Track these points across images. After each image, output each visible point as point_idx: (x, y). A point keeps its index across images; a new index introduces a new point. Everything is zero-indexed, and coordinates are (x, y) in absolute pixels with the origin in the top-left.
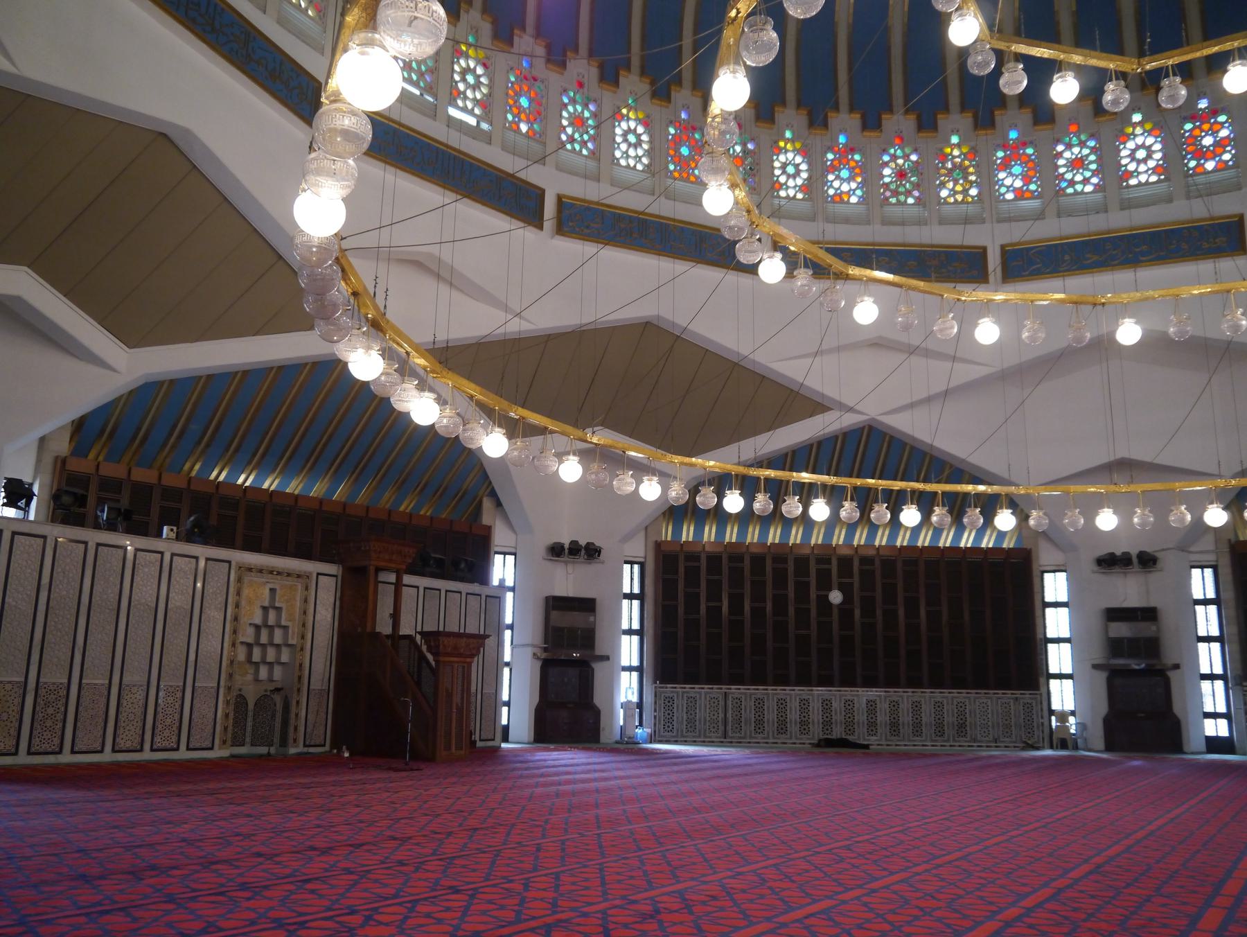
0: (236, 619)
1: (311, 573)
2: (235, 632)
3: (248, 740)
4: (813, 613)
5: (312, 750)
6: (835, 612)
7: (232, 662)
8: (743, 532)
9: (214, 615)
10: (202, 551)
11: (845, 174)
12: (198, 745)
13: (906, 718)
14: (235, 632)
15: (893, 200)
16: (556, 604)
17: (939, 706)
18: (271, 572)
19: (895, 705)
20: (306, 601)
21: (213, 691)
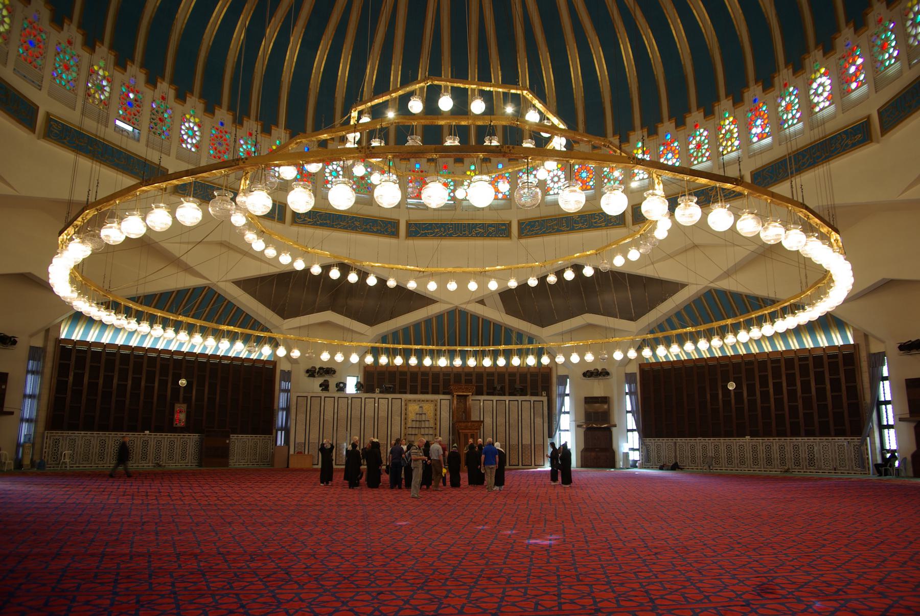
4: (720, 396)
6: (732, 393)
8: (786, 343)
9: (397, 419)
10: (390, 396)
11: (670, 156)
13: (776, 455)
15: (696, 162)
16: (589, 400)
17: (796, 447)
19: (769, 447)
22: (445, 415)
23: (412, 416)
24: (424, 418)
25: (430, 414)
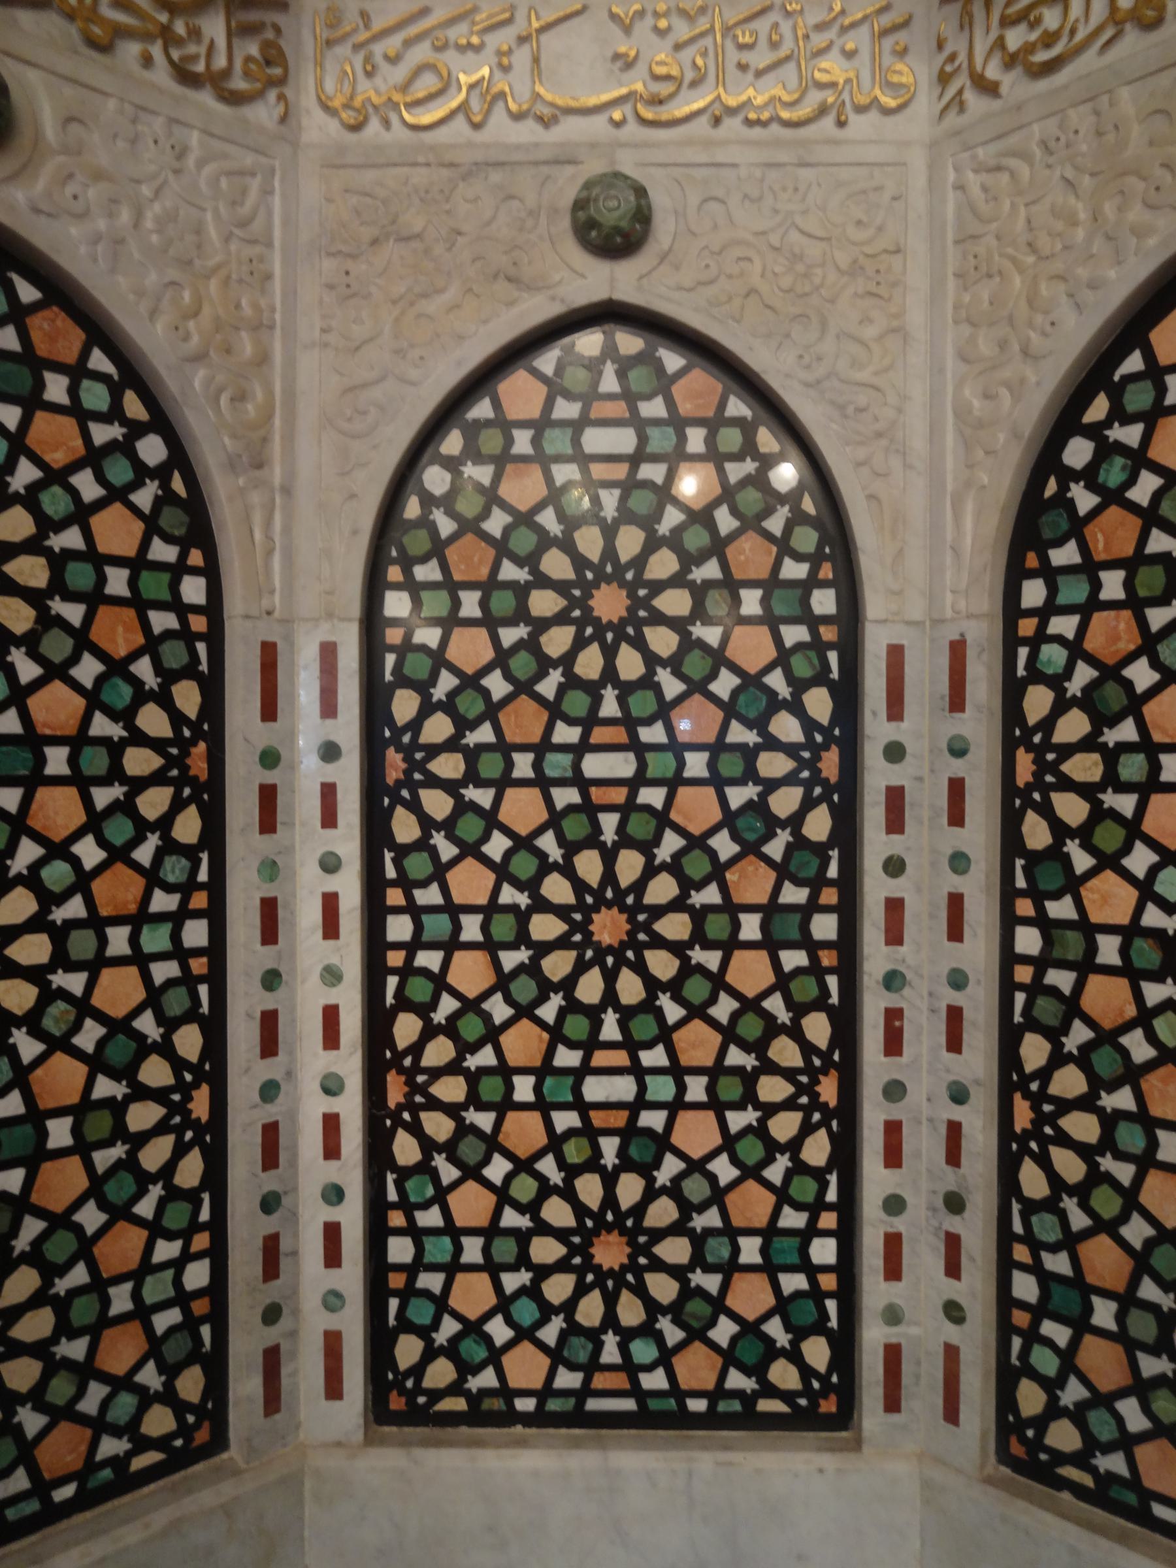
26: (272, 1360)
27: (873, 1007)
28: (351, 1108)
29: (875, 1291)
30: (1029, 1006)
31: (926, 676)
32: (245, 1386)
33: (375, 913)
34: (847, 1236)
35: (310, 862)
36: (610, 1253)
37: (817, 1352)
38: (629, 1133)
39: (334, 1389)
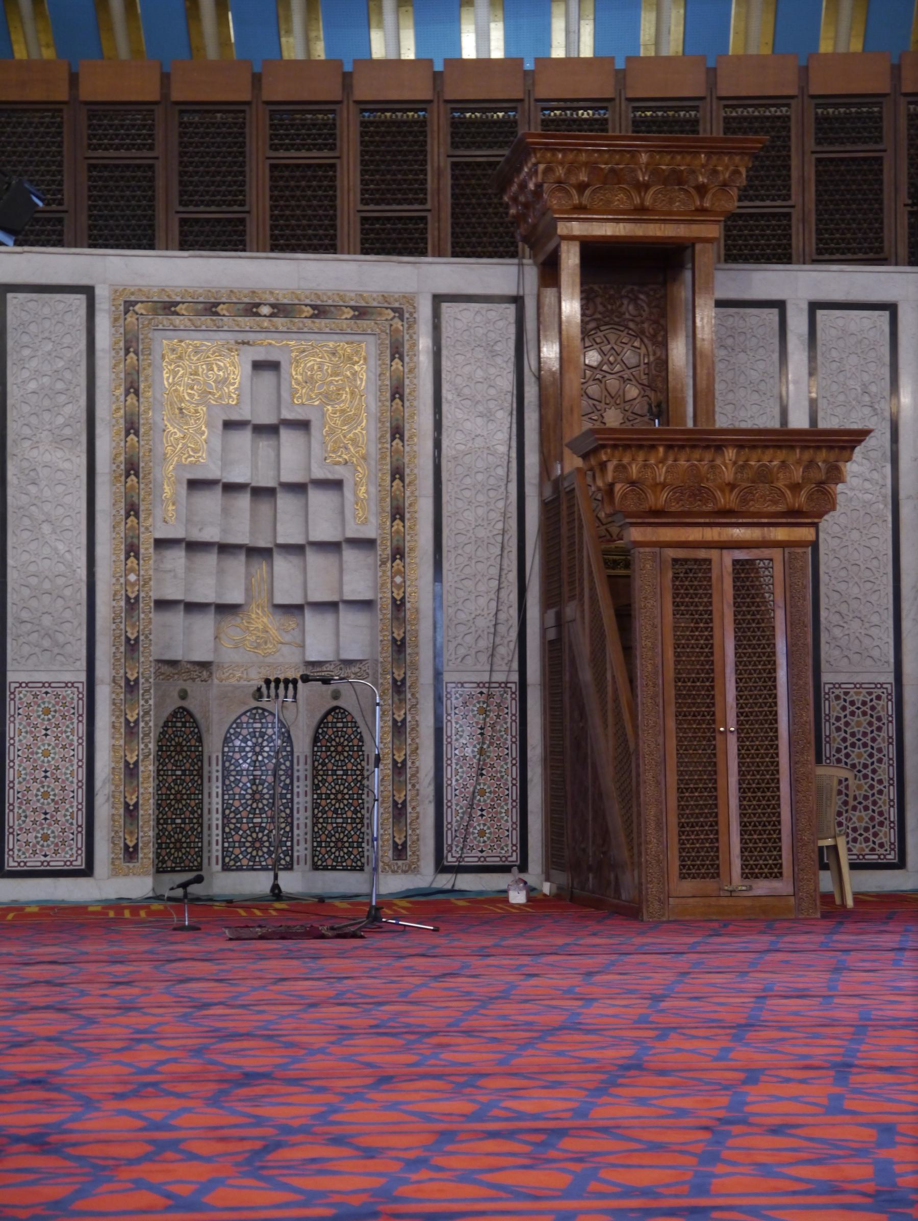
0: (132, 468)
1: (410, 299)
2: (132, 510)
3: (302, 850)
5: (466, 882)
7: (132, 605)
12: (34, 863)
14: (132, 510)
18: (251, 310)
20: (397, 392)
21: (76, 699)
22: (481, 437)
23: (185, 442)
24: (291, 458)
25: (349, 433)
26: (209, 858)
27: (295, 807)
28: (220, 822)
29: (296, 848)
30: (316, 805)
31: (302, 760)
32: (205, 861)
33: (223, 795)
34: (292, 841)
35: (216, 788)
36: (257, 845)
37: (288, 859)
38: (260, 827)
39: (217, 863)
